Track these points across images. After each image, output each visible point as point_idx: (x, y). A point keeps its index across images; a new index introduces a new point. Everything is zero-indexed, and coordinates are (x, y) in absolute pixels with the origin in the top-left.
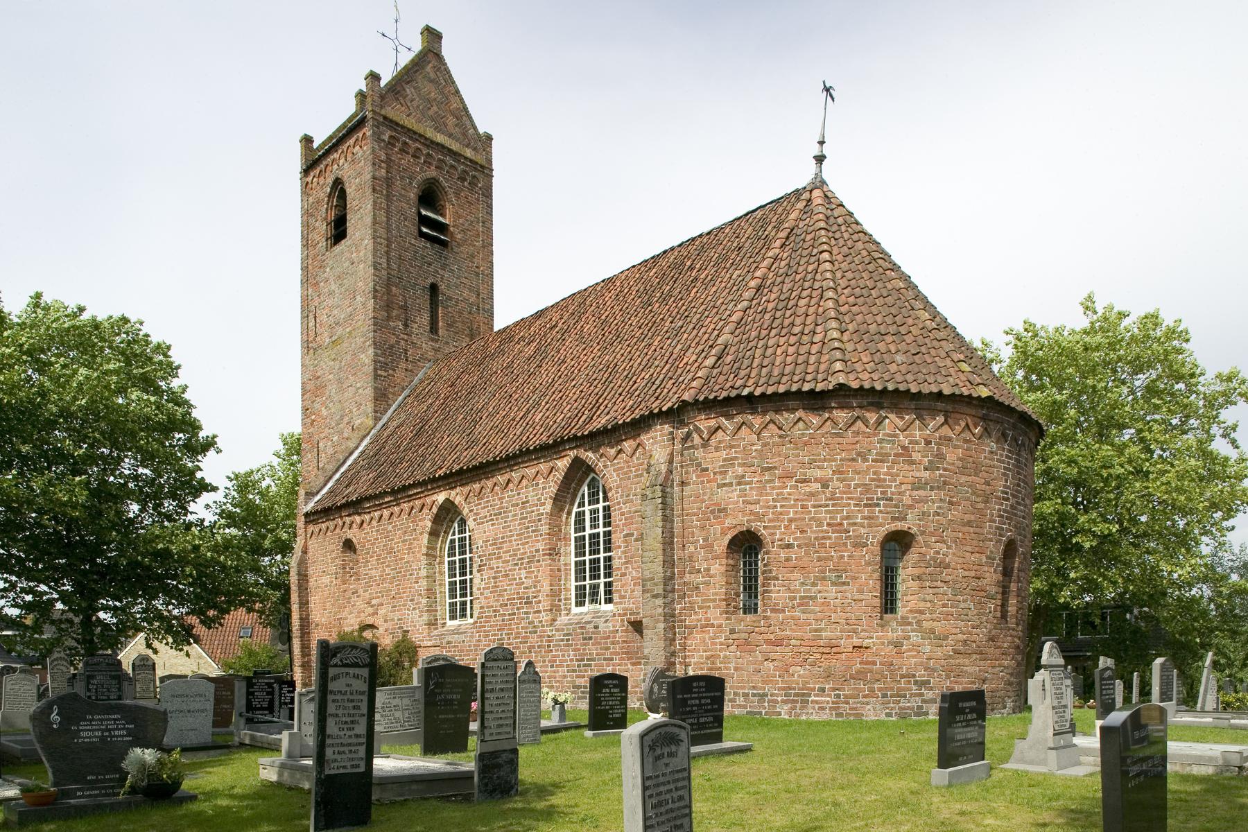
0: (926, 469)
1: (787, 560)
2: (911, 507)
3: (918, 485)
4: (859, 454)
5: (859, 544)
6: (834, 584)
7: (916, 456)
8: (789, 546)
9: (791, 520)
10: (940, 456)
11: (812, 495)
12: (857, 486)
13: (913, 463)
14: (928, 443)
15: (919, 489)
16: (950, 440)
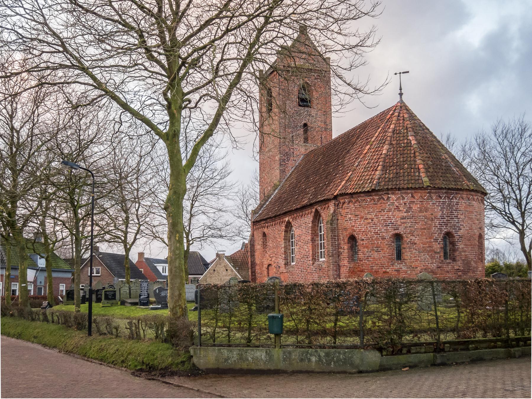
0: (405, 212)
1: (363, 244)
2: (401, 225)
3: (403, 218)
4: (382, 210)
5: (383, 238)
6: (376, 252)
7: (401, 209)
8: (363, 240)
9: (363, 232)
10: (410, 208)
11: (369, 223)
12: (382, 220)
13: (401, 211)
14: (405, 204)
15: (403, 219)
16: (414, 202)
